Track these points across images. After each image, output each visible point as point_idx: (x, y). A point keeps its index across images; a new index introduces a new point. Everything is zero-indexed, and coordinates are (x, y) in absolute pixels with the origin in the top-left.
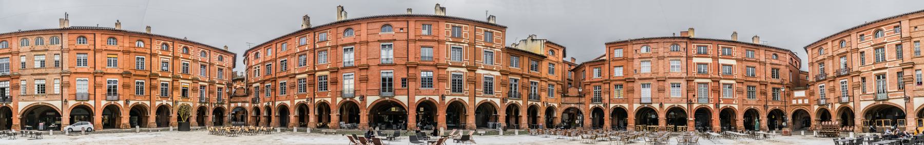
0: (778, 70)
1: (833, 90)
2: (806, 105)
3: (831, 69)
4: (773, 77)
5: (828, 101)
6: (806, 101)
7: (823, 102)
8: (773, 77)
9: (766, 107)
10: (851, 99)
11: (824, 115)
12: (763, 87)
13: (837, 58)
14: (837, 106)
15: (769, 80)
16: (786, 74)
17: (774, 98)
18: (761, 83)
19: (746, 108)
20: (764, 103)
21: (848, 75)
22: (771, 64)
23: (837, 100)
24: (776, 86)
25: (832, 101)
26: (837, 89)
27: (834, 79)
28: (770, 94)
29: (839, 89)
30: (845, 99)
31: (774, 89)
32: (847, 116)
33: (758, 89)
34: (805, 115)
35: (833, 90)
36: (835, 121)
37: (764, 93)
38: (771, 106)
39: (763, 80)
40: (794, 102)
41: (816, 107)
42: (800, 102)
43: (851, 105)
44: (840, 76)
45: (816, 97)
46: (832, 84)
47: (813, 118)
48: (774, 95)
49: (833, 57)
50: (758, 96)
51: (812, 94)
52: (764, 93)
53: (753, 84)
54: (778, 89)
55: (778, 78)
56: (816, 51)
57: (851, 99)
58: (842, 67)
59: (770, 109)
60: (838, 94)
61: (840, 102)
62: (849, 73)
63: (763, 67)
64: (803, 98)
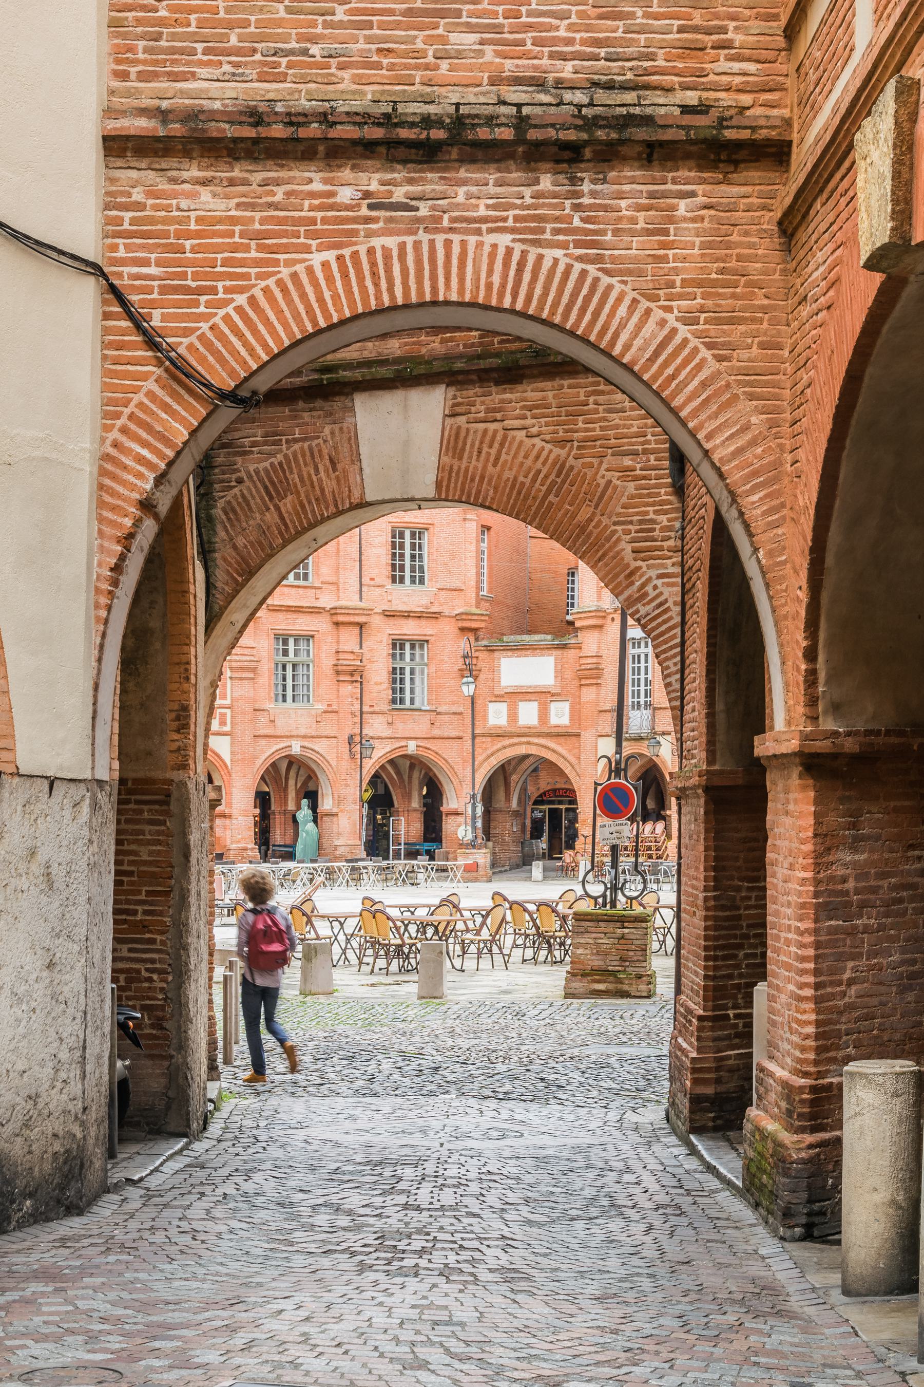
4: (397, 578)
6: (560, 714)
8: (397, 578)
9: (358, 744)
12: (349, 640)
17: (397, 699)
18: (340, 620)
19: (267, 752)
24: (410, 628)
31: (398, 644)
33: (323, 655)
34: (545, 783)
37: (351, 674)
38: (389, 736)
40: (496, 715)
42: (528, 714)
50: (324, 690)
52: (351, 674)
53: (302, 624)
54: (418, 643)
59: (380, 753)
64: (543, 696)
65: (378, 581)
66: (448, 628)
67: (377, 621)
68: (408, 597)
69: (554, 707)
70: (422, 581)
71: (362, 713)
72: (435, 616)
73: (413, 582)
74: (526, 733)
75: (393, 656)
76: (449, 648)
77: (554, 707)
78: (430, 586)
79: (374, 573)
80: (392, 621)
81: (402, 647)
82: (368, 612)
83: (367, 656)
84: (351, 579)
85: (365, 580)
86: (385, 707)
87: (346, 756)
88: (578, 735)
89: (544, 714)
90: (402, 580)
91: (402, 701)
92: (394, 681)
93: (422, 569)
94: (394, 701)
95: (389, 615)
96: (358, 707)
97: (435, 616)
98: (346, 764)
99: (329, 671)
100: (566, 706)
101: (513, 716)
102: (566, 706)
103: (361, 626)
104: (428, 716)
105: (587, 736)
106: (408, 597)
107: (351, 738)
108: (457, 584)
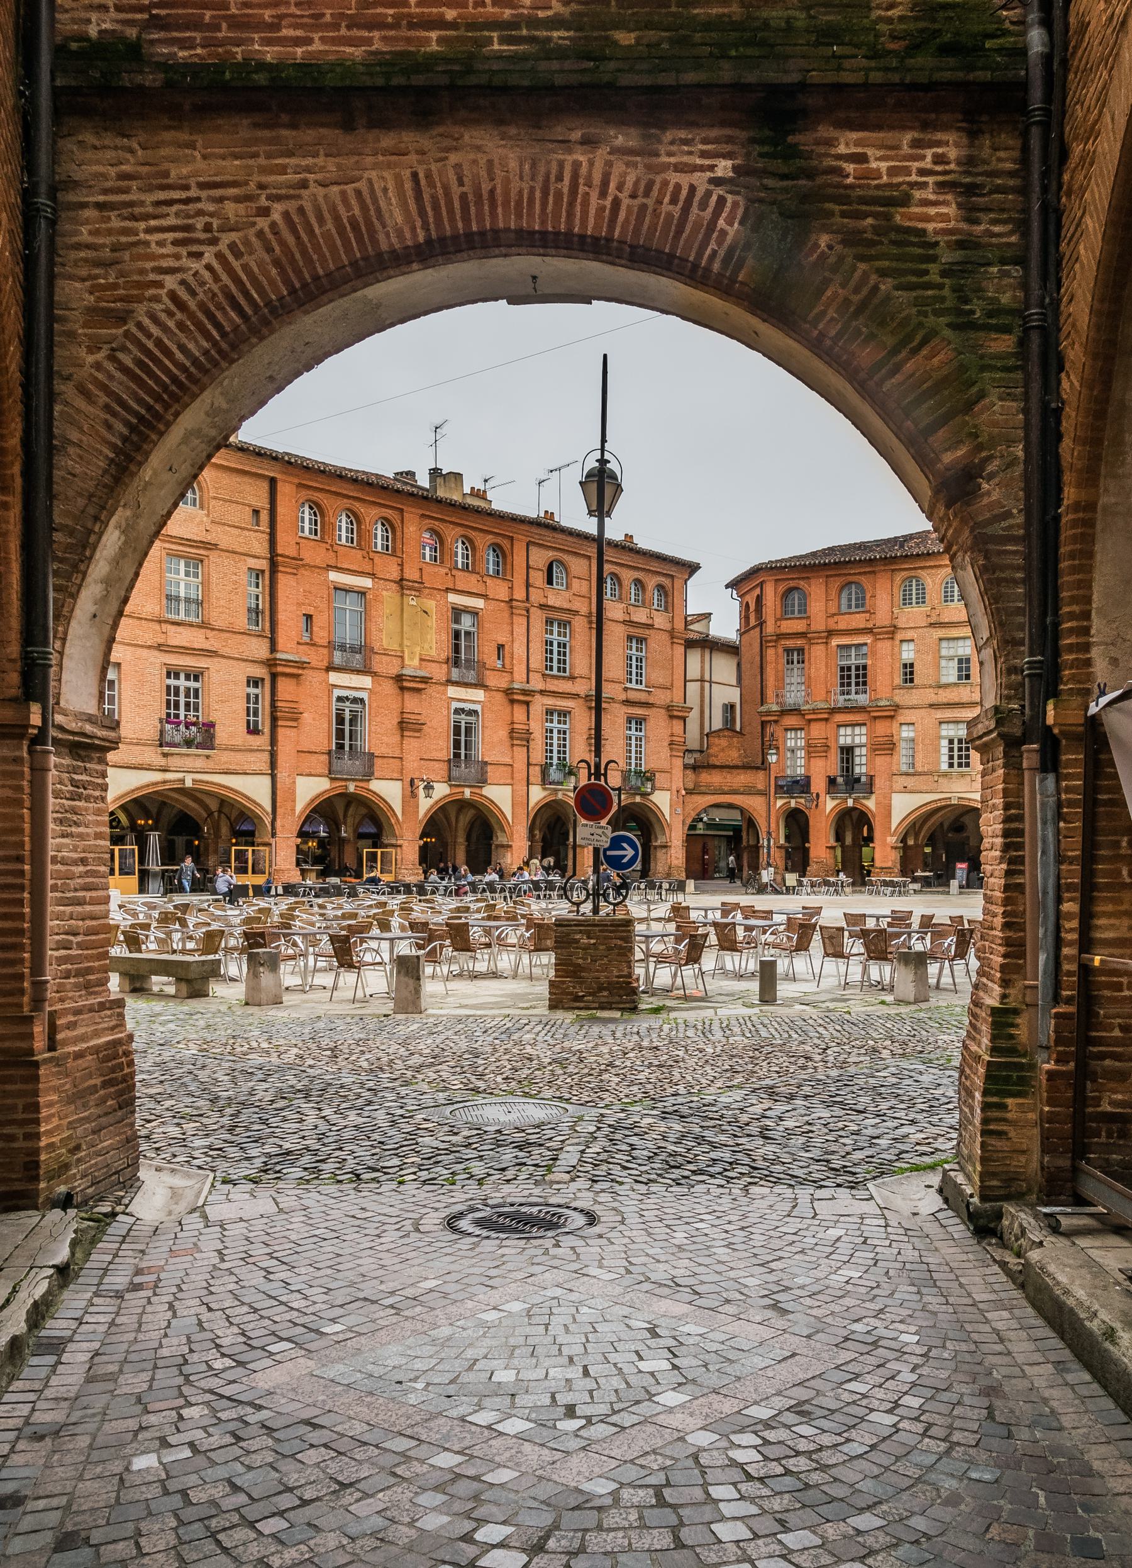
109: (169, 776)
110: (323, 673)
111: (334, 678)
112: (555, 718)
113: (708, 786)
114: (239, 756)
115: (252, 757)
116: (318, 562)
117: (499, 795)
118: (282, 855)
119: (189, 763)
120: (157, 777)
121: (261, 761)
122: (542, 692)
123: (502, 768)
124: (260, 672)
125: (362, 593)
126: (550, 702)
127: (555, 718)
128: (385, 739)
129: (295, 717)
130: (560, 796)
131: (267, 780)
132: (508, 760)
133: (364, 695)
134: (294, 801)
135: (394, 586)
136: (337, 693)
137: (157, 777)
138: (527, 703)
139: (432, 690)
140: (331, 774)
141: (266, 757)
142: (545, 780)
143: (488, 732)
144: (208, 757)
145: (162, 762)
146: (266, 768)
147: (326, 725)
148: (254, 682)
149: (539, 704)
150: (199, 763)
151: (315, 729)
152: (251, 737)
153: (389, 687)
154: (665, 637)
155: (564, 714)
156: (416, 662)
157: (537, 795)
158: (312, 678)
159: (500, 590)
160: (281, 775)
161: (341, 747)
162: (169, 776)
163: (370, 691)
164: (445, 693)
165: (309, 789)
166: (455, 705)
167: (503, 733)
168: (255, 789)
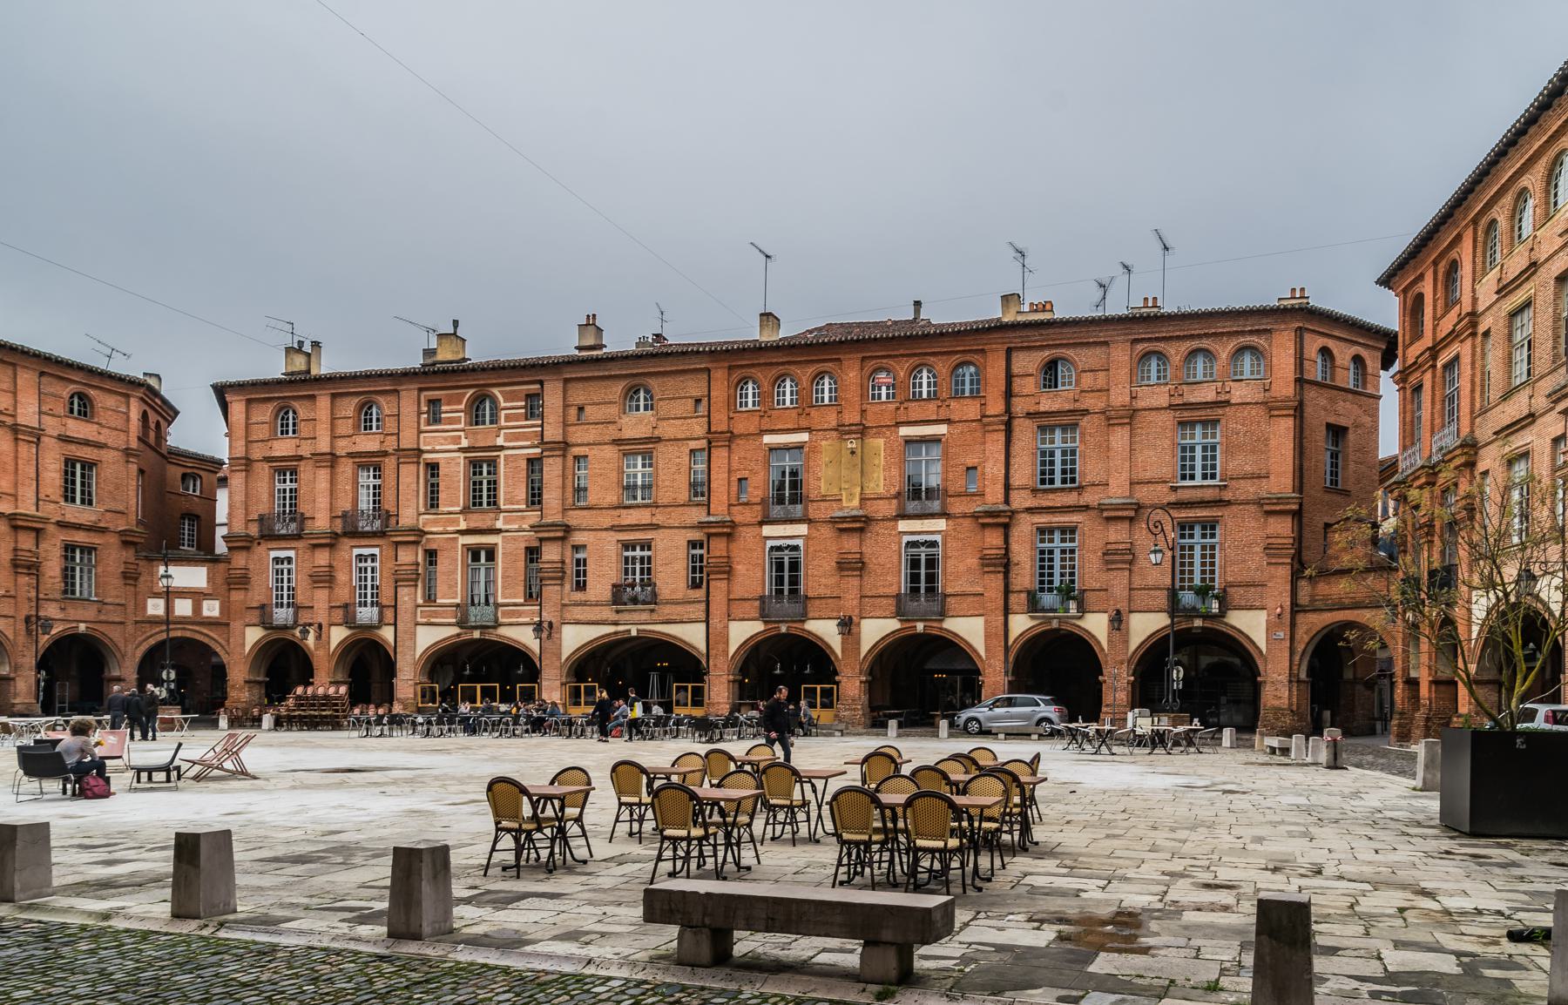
0: (88, 465)
1: (325, 579)
2: (211, 623)
3: (323, 502)
4: (69, 496)
5: (304, 617)
6: (211, 609)
7: (282, 615)
10: (389, 614)
11: (283, 665)
12: (26, 541)
13: (346, 468)
14: (338, 635)
15: (50, 511)
16: (120, 493)
20: (26, 610)
21: (381, 534)
22: (65, 439)
23: (338, 615)
24: (80, 537)
25: (321, 616)
26: (341, 577)
27: (332, 541)
28: (53, 568)
29: (347, 578)
30: (366, 614)
31: (69, 548)
32: (368, 669)
35: (325, 579)
36: (326, 684)
39: (27, 507)
41: (254, 635)
42: (183, 608)
43: (387, 634)
44: (354, 534)
45: (256, 596)
46: (322, 558)
47: (238, 673)
48: (68, 575)
49: (332, 460)
51: (241, 581)
54: (88, 550)
55: (87, 501)
56: (264, 413)
57: (389, 614)
58: (366, 503)
60: (343, 594)
61: (349, 621)
62: (385, 528)
63: (26, 451)
64: (197, 596)
65: (53, 498)
66: (113, 540)
67: (51, 528)
68: (76, 512)
69: (206, 604)
70: (90, 503)
71: (38, 599)
72: (103, 531)
73: (83, 501)
74: (183, 621)
75: (66, 558)
76: (113, 558)
77: (206, 604)
78: (98, 508)
79: (49, 491)
80: (65, 531)
81: (73, 551)
82: (45, 520)
83: (43, 555)
84: (28, 494)
85: (42, 496)
86: (58, 596)
87: (23, 633)
88: (228, 625)
89: (197, 608)
90: (73, 500)
91: (73, 592)
92: (66, 577)
93: (90, 494)
94: (65, 592)
95: (62, 525)
96: (33, 594)
97: (103, 531)
98: (22, 639)
99: (7, 564)
100: (217, 604)
101: (169, 608)
102: (217, 604)
103: (38, 531)
104: (95, 606)
105: (236, 625)
106: (76, 512)
107: (28, 620)
108: (121, 508)
109: (621, 628)
110: (755, 530)
111: (767, 530)
112: (1057, 536)
113: (1326, 598)
114: (679, 608)
115: (690, 608)
116: (752, 429)
117: (969, 629)
118: (720, 693)
119: (636, 617)
120: (611, 629)
121: (698, 611)
122: (1030, 510)
123: (971, 599)
124: (697, 535)
125: (799, 447)
126: (1043, 519)
127: (1057, 536)
128: (823, 580)
129: (728, 571)
130: (1055, 624)
131: (703, 626)
132: (979, 589)
133: (800, 542)
134: (727, 643)
135: (834, 434)
136: (770, 543)
137: (611, 629)
138: (1006, 527)
139: (877, 528)
140: (763, 616)
141: (703, 606)
142: (1033, 606)
143: (950, 563)
144: (652, 611)
145: (615, 617)
146: (703, 617)
147: (759, 574)
148: (693, 544)
149: (1024, 528)
150: (645, 616)
151: (752, 577)
152: (691, 592)
153: (826, 532)
154: (1261, 411)
155: (1069, 531)
156: (856, 502)
157: (1021, 624)
158: (746, 534)
159: (971, 410)
160: (714, 621)
161: (780, 592)
162: (621, 628)
163: (807, 538)
164: (895, 528)
165: (742, 631)
166: (906, 539)
167: (973, 561)
168: (693, 635)
